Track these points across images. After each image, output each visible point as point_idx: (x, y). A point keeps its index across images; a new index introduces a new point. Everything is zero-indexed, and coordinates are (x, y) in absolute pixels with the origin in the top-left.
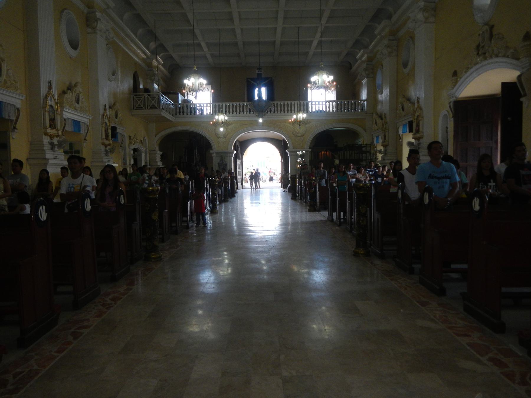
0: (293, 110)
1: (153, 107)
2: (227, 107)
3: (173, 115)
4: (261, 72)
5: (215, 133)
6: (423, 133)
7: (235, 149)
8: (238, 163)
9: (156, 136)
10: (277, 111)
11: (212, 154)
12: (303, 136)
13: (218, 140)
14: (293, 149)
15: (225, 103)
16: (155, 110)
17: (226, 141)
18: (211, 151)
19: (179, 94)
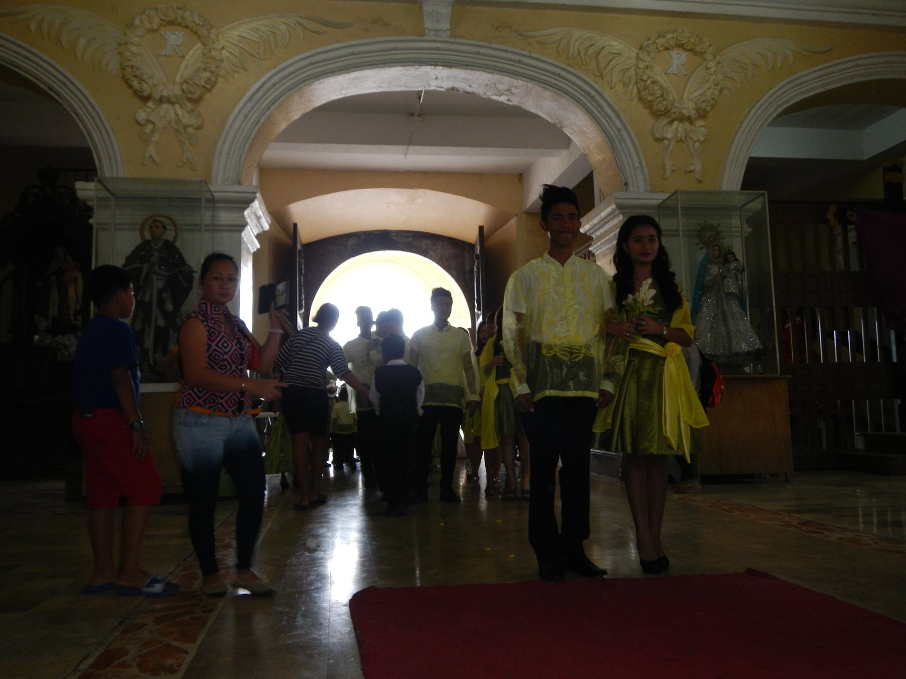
5: (123, 68)
12: (702, 114)
13: (142, 116)
14: (653, 191)
17: (199, 128)
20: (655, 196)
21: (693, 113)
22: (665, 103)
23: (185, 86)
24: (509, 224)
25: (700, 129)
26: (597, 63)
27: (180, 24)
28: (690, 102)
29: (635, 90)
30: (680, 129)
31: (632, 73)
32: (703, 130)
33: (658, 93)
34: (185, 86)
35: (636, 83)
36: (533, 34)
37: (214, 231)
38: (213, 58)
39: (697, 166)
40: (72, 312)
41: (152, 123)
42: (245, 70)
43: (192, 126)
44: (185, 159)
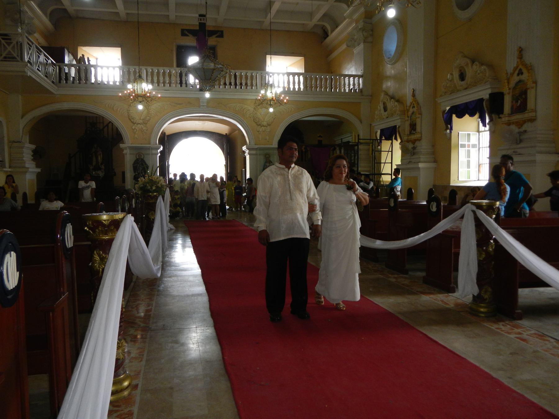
0: (254, 84)
1: (9, 58)
2: (149, 74)
3: (53, 82)
5: (129, 116)
6: (535, 111)
9: (22, 118)
11: (122, 150)
12: (269, 125)
13: (133, 128)
14: (255, 145)
15: (146, 67)
16: (15, 63)
17: (147, 130)
18: (122, 146)
19: (66, 50)
20: (256, 146)
22: (259, 123)
23: (144, 121)
25: (268, 129)
26: (243, 112)
30: (264, 129)
31: (252, 114)
32: (269, 129)
33: (258, 120)
34: (144, 121)
38: (150, 114)
39: (268, 138)
40: (100, 164)
42: (157, 116)
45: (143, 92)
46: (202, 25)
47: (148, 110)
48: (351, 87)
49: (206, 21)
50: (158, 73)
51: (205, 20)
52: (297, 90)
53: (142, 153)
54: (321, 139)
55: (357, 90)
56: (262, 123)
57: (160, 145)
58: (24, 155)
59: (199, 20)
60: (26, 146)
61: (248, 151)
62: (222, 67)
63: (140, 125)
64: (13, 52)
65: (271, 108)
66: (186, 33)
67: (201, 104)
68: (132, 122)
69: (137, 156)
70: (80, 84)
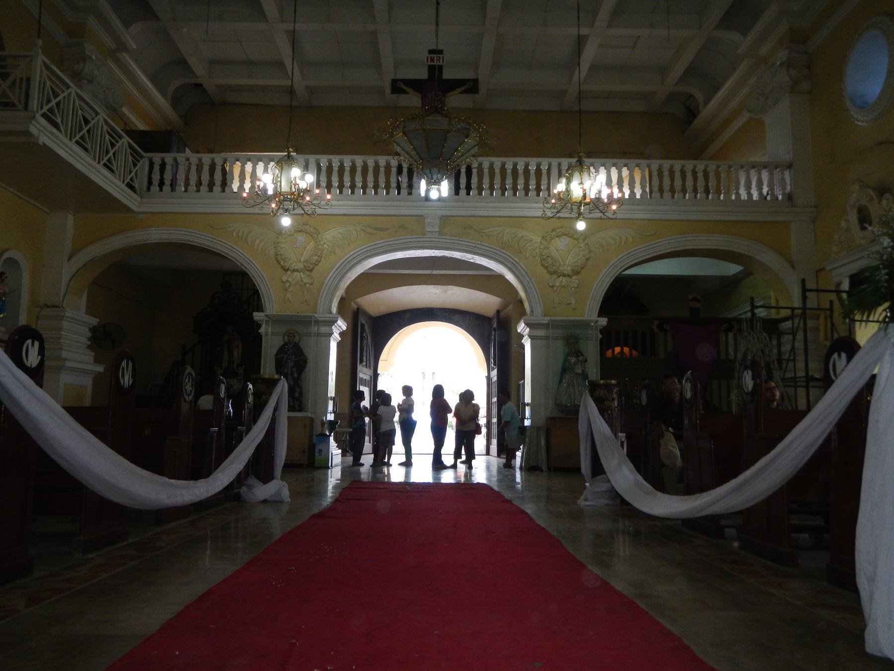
3: (130, 186)
4: (441, 63)
7: (341, 311)
8: (361, 375)
9: (69, 260)
10: (492, 188)
13: (284, 278)
14: (545, 316)
17: (311, 284)
18: (257, 316)
21: (570, 273)
22: (554, 268)
24: (508, 308)
27: (303, 232)
28: (569, 267)
29: (539, 260)
30: (563, 281)
31: (538, 250)
32: (577, 281)
33: (550, 262)
34: (305, 264)
35: (539, 256)
36: (484, 231)
37: (318, 336)
39: (573, 301)
40: (235, 365)
41: (290, 282)
43: (308, 283)
44: (304, 300)
45: (293, 187)
46: (435, 71)
47: (316, 242)
48: (765, 190)
49: (443, 62)
50: (341, 169)
51: (441, 61)
52: (638, 196)
53: (297, 332)
54: (697, 305)
55: (780, 197)
56: (561, 268)
57: (337, 316)
58: (62, 333)
59: (429, 61)
60: (67, 314)
61: (528, 329)
62: (467, 126)
63: (298, 273)
64: (10, 94)
65: (581, 220)
66: (402, 86)
67: (429, 230)
68: (282, 267)
69: (286, 337)
70: (185, 193)
